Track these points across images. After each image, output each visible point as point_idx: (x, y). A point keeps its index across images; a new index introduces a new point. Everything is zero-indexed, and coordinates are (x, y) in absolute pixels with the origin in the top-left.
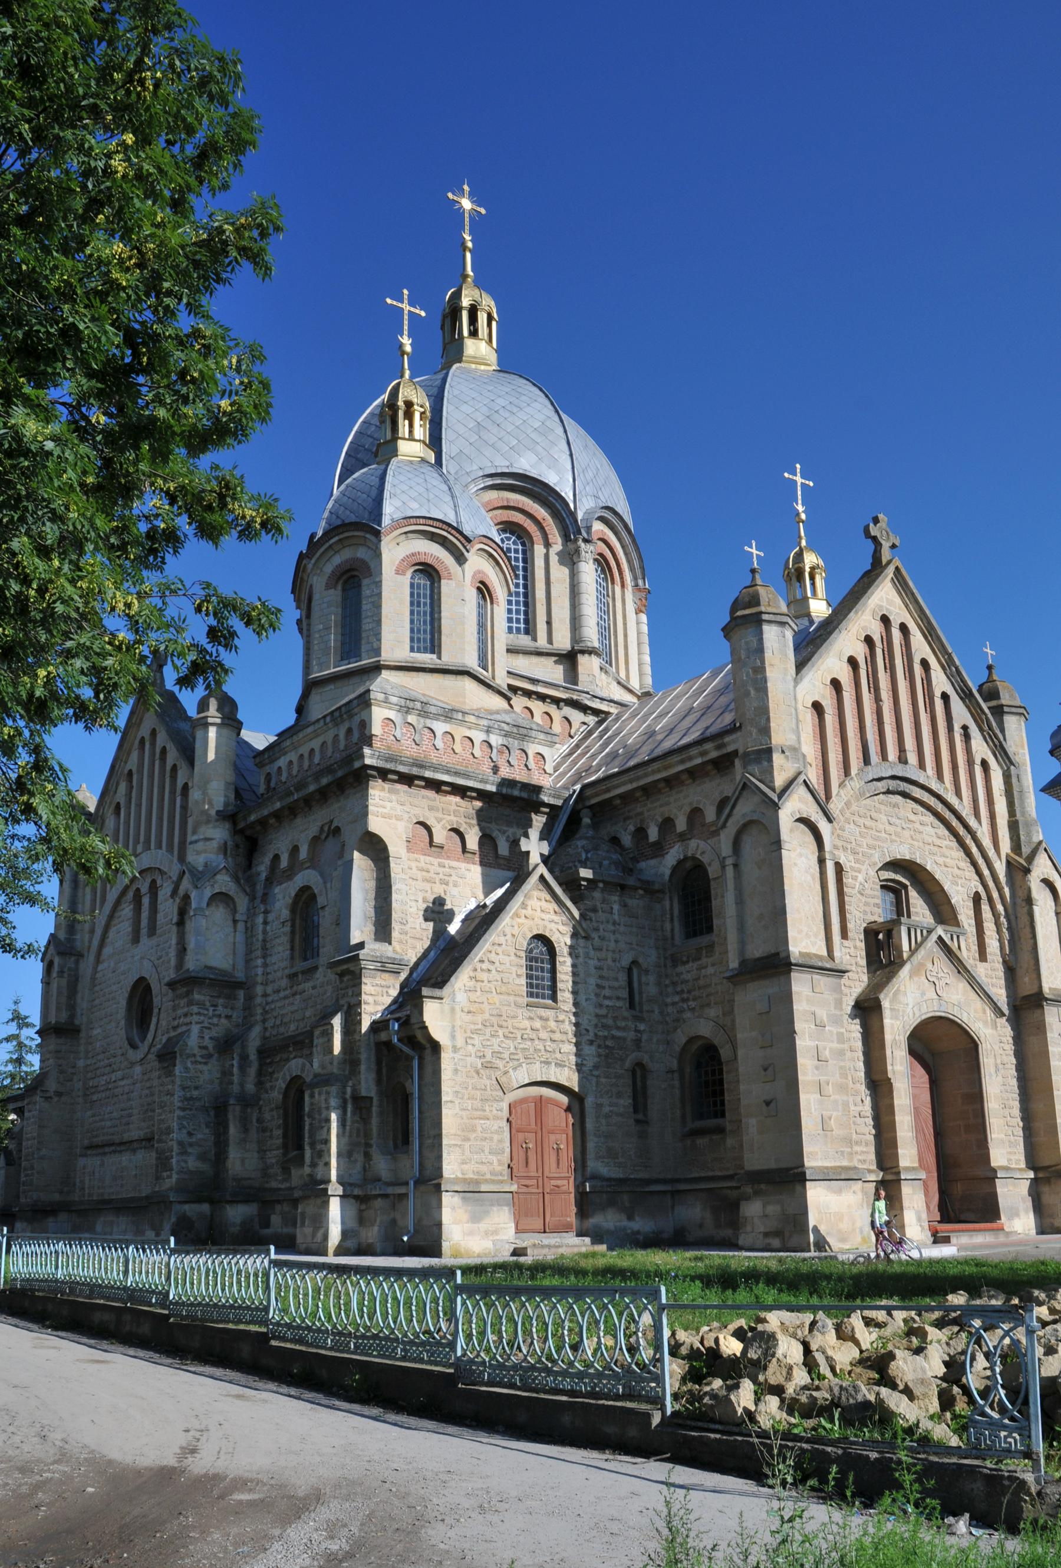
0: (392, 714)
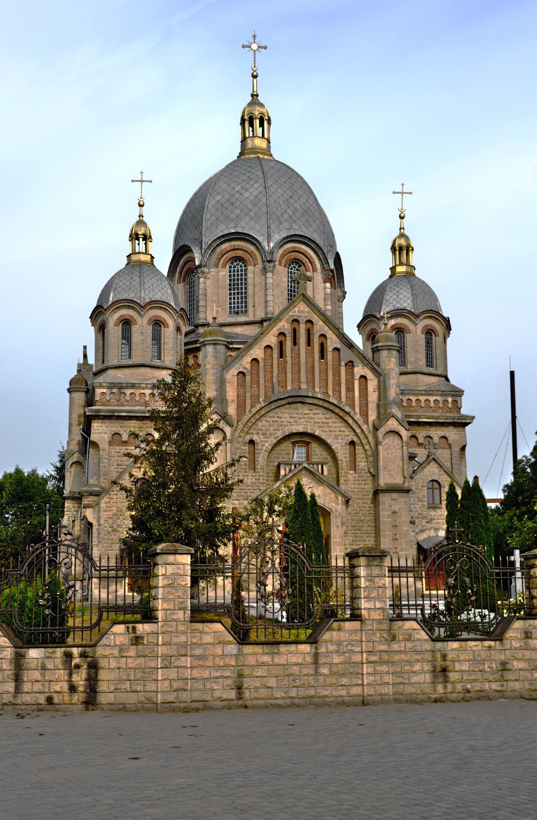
0: (105, 390)
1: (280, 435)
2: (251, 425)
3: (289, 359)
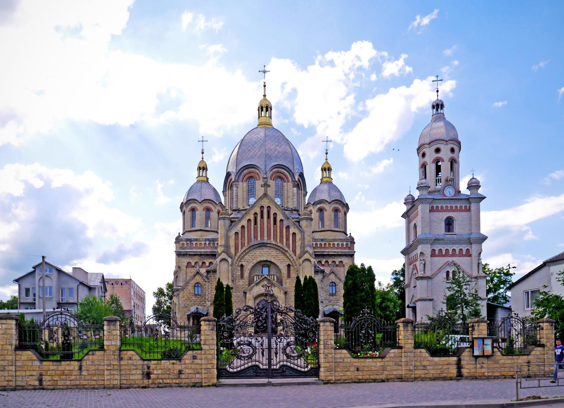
1: (255, 262)
2: (241, 257)
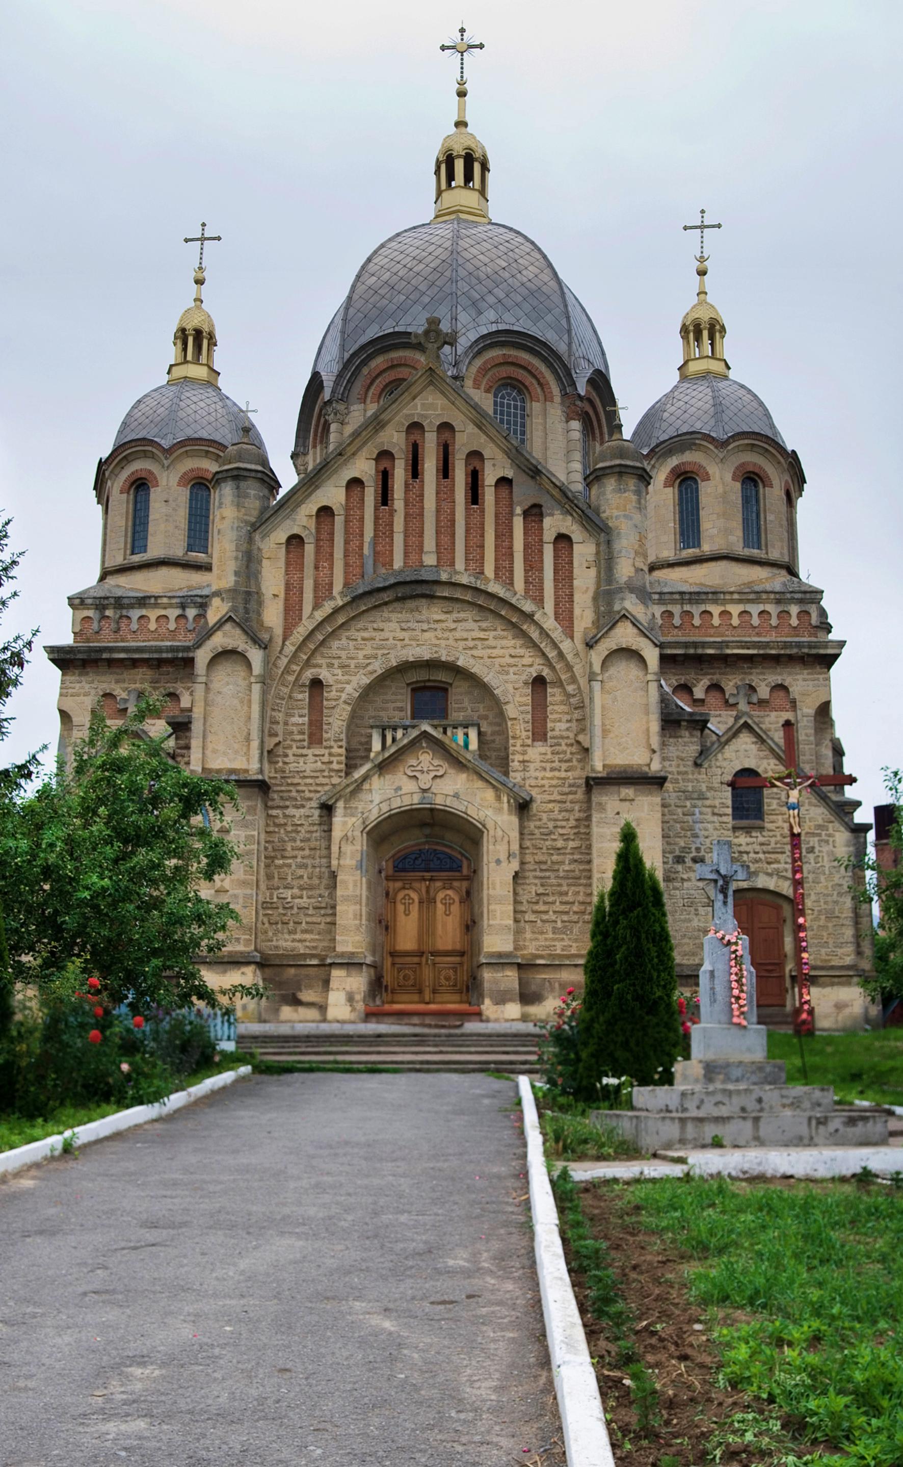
1: (378, 667)
3: (398, 504)
